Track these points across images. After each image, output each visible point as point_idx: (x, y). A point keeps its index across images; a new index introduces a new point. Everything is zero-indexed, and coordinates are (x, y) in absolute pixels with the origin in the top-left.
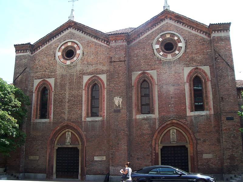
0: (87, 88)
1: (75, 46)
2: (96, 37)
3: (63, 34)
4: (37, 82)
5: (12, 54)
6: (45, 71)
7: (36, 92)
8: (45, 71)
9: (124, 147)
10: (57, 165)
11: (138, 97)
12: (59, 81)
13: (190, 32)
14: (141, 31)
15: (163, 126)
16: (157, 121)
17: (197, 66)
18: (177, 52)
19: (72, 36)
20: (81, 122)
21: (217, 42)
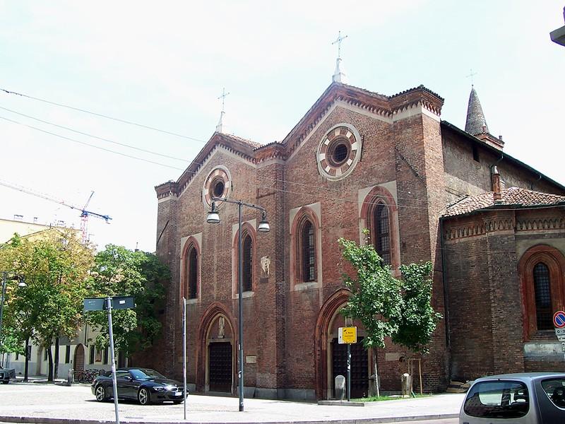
0: (236, 244)
1: (224, 175)
2: (247, 156)
3: (210, 158)
4: (184, 241)
5: (153, 202)
6: (192, 223)
7: (184, 257)
8: (192, 223)
9: (272, 340)
10: (210, 372)
11: (297, 253)
12: (206, 236)
13: (369, 119)
14: (301, 133)
15: (330, 301)
16: (321, 293)
17: (379, 183)
18: (349, 162)
19: (220, 159)
20: (231, 302)
21: (400, 132)
